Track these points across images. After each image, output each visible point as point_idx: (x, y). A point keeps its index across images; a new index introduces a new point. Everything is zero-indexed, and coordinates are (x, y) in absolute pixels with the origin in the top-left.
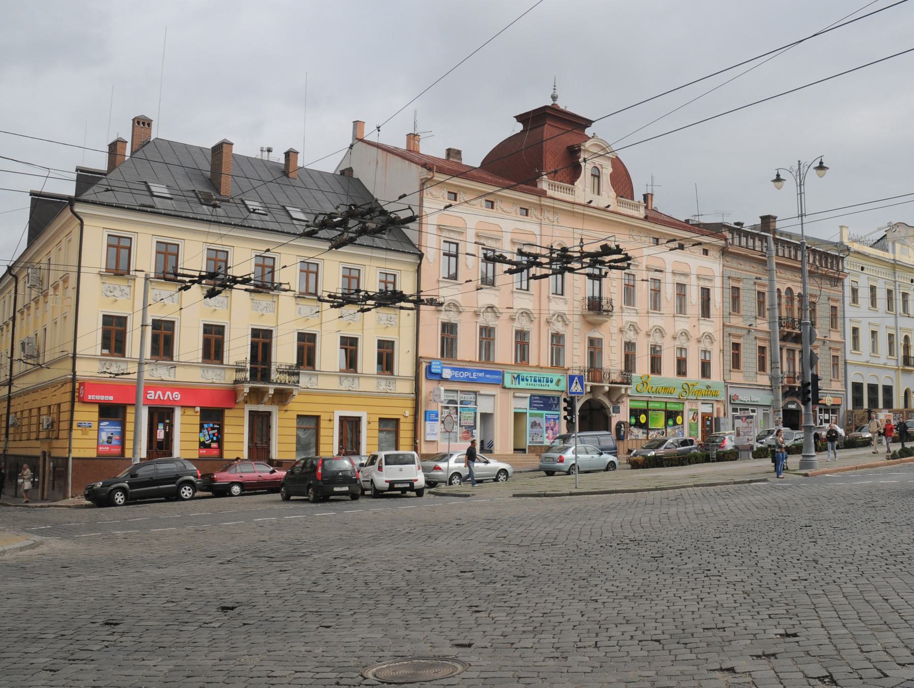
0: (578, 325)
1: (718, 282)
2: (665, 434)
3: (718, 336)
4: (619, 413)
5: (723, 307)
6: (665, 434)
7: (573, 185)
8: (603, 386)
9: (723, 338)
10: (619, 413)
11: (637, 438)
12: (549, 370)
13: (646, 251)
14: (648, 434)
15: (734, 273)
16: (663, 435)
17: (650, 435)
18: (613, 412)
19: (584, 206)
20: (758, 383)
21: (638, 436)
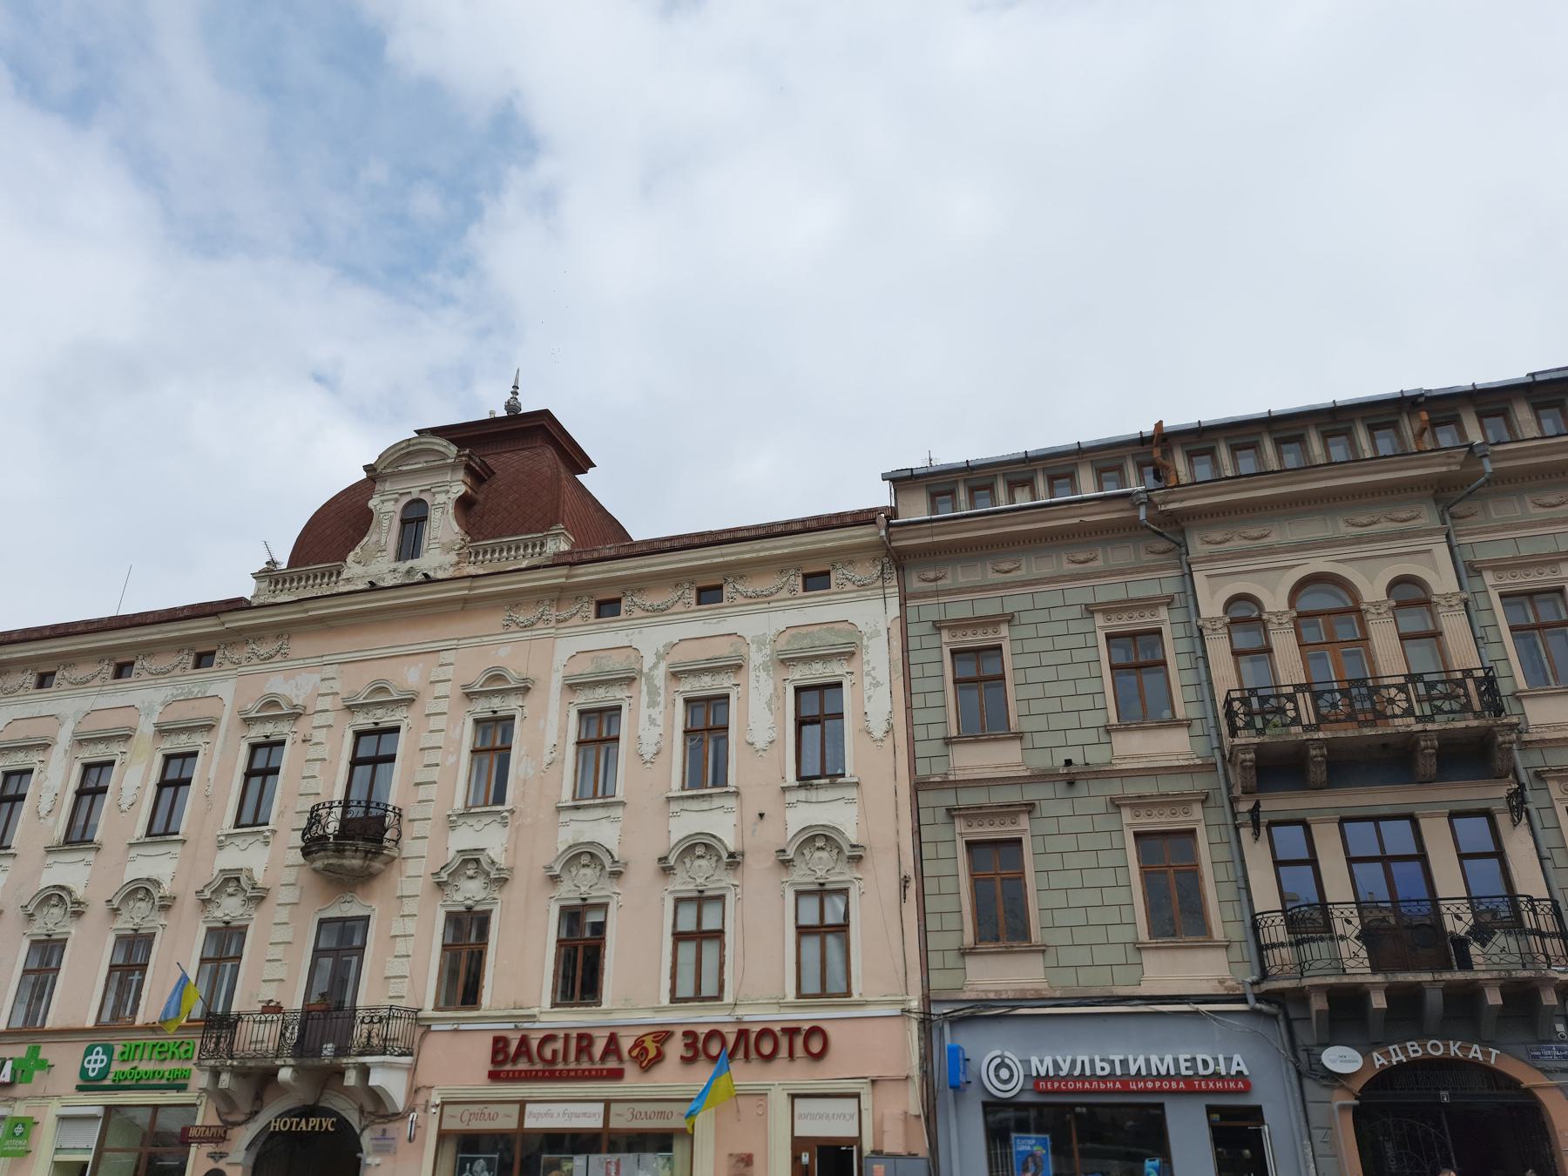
1: (879, 657)
5: (910, 723)
9: (917, 832)
15: (959, 609)
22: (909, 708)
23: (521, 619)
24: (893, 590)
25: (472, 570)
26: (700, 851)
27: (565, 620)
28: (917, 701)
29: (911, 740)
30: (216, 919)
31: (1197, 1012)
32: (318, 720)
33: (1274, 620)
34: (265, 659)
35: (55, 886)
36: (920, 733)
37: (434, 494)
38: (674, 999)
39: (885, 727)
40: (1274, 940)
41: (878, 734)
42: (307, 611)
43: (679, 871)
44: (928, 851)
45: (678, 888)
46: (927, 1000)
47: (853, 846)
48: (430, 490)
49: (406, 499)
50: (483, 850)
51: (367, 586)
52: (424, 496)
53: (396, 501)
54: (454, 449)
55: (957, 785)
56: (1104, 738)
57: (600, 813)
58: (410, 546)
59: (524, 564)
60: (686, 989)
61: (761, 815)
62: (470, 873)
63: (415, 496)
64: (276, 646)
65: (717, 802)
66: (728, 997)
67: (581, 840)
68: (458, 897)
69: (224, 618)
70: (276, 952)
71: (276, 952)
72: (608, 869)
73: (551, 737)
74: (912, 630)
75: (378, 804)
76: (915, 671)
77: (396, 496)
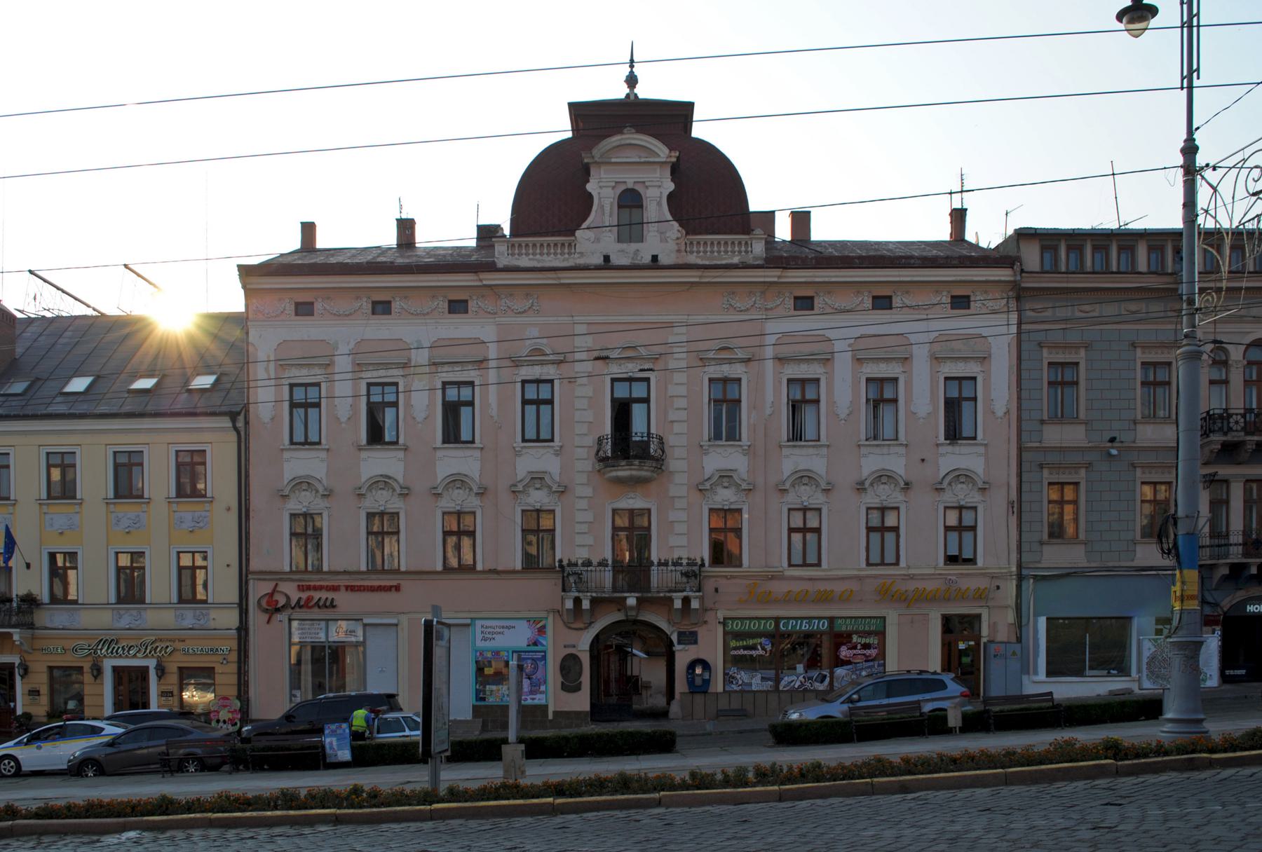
0: (588, 491)
2: (828, 679)
3: (1006, 473)
4: (696, 642)
5: (1019, 409)
6: (828, 679)
7: (573, 234)
8: (625, 598)
9: (1020, 475)
10: (696, 642)
11: (747, 688)
12: (518, 576)
13: (775, 327)
14: (777, 680)
16: (822, 682)
17: (783, 683)
18: (679, 643)
19: (598, 268)
20: (1137, 563)
21: (750, 684)
22: (1019, 398)
23: (738, 305)
24: (1014, 317)
25: (692, 259)
26: (884, 479)
27: (771, 309)
28: (1024, 394)
29: (1019, 419)
30: (528, 504)
31: (1158, 575)
32: (578, 367)
33: (1234, 364)
34: (519, 313)
35: (381, 475)
36: (1025, 415)
37: (647, 187)
38: (868, 564)
39: (1004, 410)
40: (1204, 544)
41: (1000, 413)
42: (559, 278)
43: (870, 491)
44: (1025, 487)
45: (868, 501)
46: (1020, 566)
47: (984, 483)
48: (644, 182)
49: (623, 188)
50: (736, 470)
51: (600, 261)
52: (639, 188)
53: (613, 188)
54: (666, 150)
55: (1047, 450)
56: (1132, 426)
57: (811, 451)
58: (631, 229)
59: (736, 260)
60: (875, 558)
61: (923, 460)
62: (726, 484)
63: (630, 186)
64: (528, 304)
65: (893, 450)
66: (903, 563)
67: (799, 468)
68: (718, 498)
69: (482, 276)
70: (584, 528)
71: (584, 528)
72: (398, 492)
73: (769, 396)
74: (1024, 346)
75: (636, 434)
76: (1024, 375)
77: (613, 184)
